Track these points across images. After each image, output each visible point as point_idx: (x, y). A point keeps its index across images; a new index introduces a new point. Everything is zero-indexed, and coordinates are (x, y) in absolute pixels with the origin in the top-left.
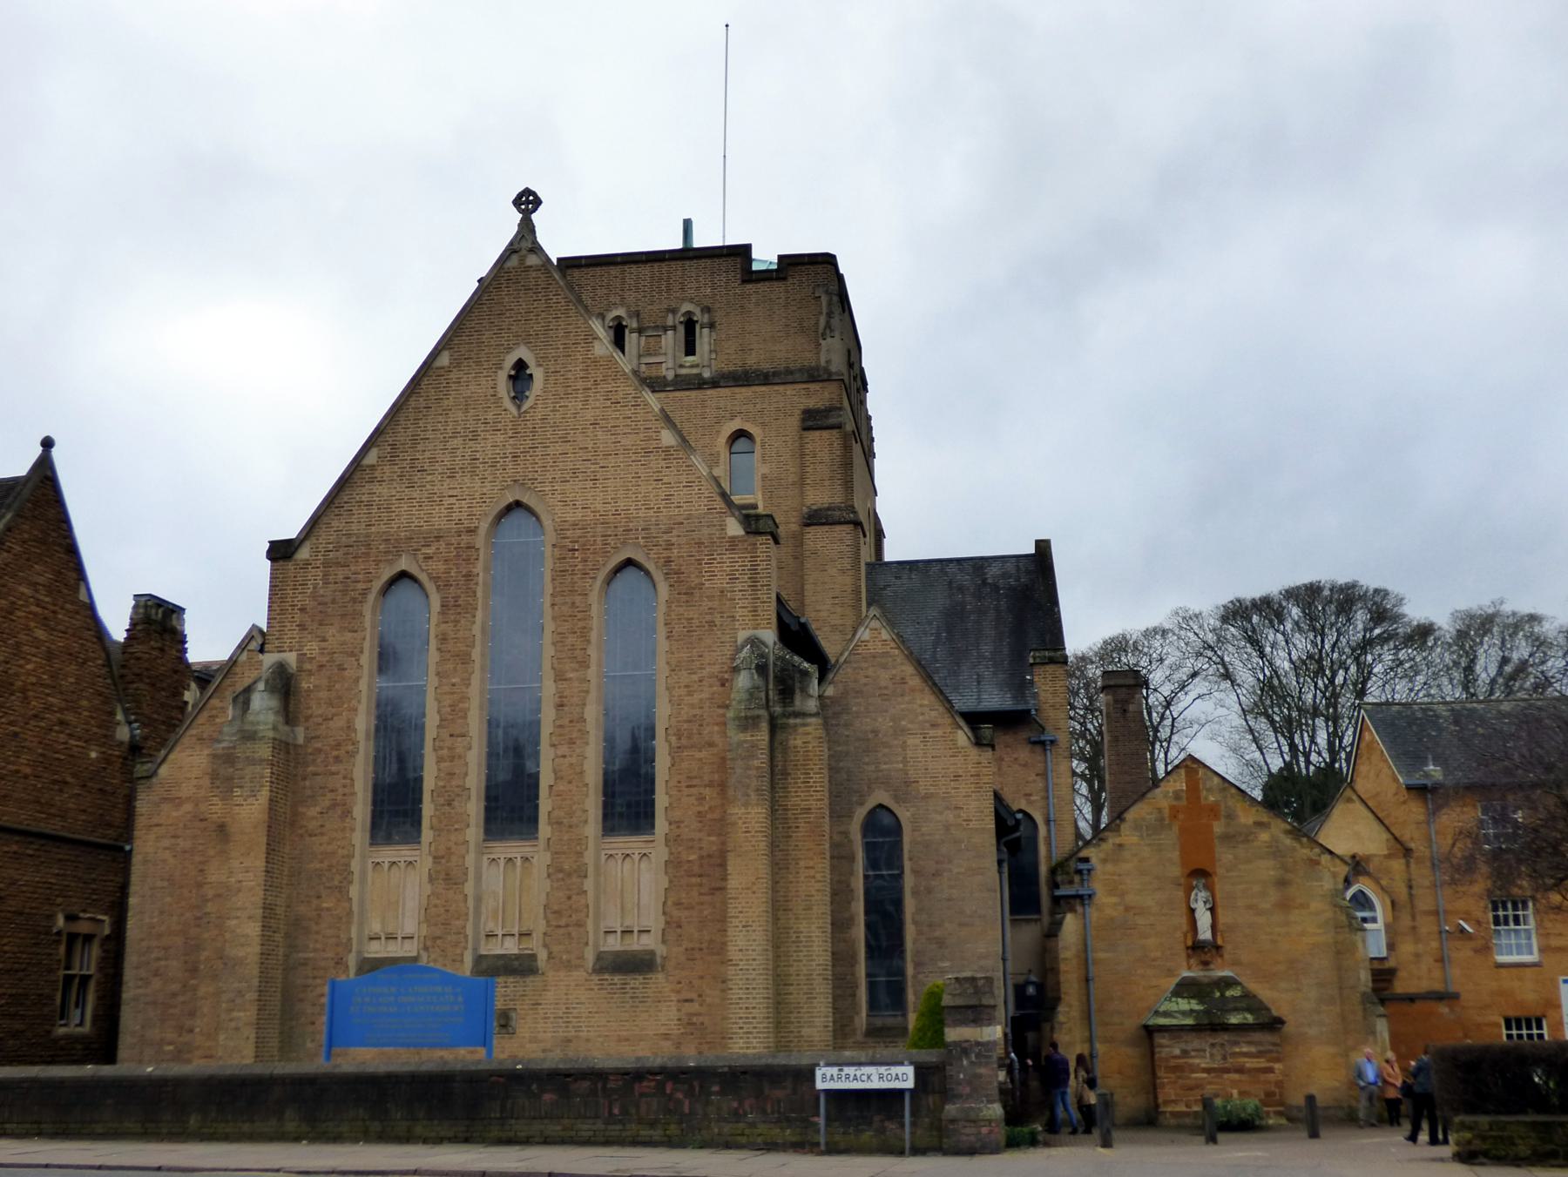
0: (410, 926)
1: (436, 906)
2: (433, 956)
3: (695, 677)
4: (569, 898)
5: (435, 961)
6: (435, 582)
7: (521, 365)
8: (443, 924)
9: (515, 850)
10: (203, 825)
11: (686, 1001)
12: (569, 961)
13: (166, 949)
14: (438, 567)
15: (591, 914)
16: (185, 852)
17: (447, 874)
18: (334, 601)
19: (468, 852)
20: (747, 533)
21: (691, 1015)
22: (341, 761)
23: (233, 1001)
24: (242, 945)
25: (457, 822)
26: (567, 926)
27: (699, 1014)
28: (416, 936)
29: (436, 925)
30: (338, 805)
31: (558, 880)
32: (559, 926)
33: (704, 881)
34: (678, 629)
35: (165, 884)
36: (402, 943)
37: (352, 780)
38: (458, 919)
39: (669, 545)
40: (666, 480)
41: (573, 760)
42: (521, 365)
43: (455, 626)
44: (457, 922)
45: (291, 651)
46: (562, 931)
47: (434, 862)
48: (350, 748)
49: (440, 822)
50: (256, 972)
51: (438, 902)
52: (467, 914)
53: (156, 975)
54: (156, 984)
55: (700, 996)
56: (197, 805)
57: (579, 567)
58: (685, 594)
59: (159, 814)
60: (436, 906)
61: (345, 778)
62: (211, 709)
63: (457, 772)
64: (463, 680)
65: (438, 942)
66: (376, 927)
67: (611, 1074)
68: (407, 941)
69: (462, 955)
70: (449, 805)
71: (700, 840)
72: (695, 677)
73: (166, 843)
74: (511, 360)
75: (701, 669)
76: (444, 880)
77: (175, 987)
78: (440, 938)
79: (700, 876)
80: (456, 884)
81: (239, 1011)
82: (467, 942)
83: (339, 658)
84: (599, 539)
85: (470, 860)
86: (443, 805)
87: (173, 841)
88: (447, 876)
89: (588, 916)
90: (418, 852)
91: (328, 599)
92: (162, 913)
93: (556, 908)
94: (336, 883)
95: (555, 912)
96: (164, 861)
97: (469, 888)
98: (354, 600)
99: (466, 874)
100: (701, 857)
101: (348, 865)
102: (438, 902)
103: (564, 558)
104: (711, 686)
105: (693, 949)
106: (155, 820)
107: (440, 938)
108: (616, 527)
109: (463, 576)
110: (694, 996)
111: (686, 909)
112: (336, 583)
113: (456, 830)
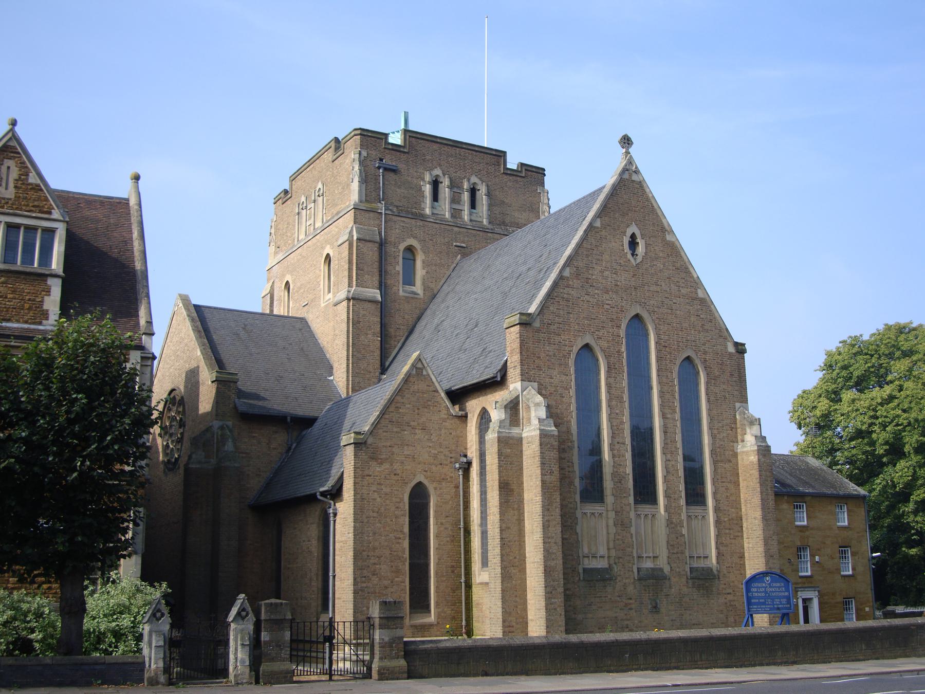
0: (603, 551)
1: (618, 540)
2: (619, 569)
4: (677, 538)
5: (620, 570)
7: (633, 236)
8: (622, 550)
9: (647, 510)
10: (396, 478)
11: (728, 594)
12: (679, 572)
15: (687, 547)
17: (622, 522)
19: (631, 510)
20: (737, 352)
21: (730, 601)
22: (566, 452)
23: (551, 593)
24: (553, 559)
25: (624, 493)
26: (677, 553)
27: (734, 601)
28: (606, 556)
34: (712, 398)
35: (375, 515)
38: (629, 547)
39: (705, 353)
41: (673, 463)
42: (633, 236)
43: (615, 380)
44: (629, 549)
45: (535, 382)
46: (675, 556)
48: (570, 444)
50: (561, 576)
51: (619, 537)
54: (375, 580)
55: (734, 591)
56: (392, 465)
57: (668, 356)
59: (369, 469)
61: (568, 462)
62: (396, 403)
64: (621, 412)
65: (621, 559)
68: (648, 559)
69: (632, 567)
70: (620, 482)
71: (728, 510)
73: (374, 488)
74: (629, 233)
76: (621, 525)
77: (386, 583)
78: (621, 558)
79: (730, 529)
81: (555, 598)
82: (634, 560)
83: (560, 390)
84: (676, 343)
85: (632, 515)
87: (379, 486)
88: (622, 524)
89: (685, 548)
90: (603, 508)
91: (550, 354)
92: (374, 534)
94: (569, 524)
95: (671, 546)
96: (374, 499)
97: (633, 530)
99: (631, 522)
100: (729, 520)
101: (575, 513)
102: (619, 537)
104: (727, 430)
105: (729, 567)
106: (366, 472)
107: (621, 558)
110: (731, 591)
112: (554, 344)
113: (625, 497)
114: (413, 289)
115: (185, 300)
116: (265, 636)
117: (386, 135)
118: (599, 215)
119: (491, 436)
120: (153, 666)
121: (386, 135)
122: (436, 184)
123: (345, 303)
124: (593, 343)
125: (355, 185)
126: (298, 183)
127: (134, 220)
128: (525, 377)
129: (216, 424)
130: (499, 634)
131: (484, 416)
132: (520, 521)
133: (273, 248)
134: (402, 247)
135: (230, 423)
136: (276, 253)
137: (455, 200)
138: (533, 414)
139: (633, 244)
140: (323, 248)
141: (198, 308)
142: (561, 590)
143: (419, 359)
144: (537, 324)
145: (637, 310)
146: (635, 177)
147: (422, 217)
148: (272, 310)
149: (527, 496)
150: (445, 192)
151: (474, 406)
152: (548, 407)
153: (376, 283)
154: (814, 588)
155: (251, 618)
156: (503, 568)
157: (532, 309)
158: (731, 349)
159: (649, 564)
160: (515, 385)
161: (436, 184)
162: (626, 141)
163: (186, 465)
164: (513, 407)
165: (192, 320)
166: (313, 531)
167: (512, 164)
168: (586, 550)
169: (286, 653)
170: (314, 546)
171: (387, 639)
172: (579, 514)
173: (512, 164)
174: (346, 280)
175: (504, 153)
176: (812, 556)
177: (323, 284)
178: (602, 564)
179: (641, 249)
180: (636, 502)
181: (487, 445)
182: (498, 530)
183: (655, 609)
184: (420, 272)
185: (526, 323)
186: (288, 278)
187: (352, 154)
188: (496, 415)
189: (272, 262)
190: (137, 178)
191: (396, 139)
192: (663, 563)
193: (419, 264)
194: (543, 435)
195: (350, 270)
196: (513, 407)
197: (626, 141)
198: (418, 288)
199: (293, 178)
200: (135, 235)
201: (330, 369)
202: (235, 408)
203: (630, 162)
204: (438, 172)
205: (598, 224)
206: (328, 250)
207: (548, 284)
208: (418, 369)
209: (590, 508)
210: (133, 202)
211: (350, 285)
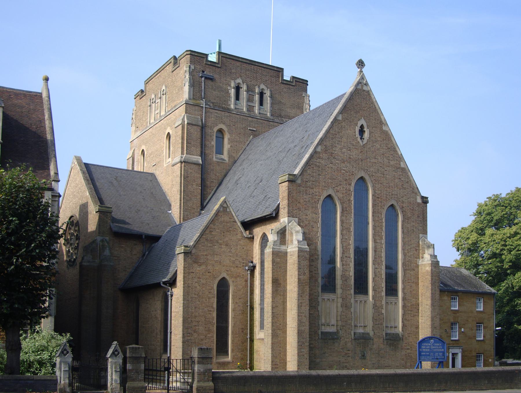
0: (333, 321)
1: (343, 315)
2: (343, 332)
3: (409, 247)
4: (379, 315)
5: (343, 334)
6: (340, 201)
7: (362, 127)
8: (345, 321)
9: (361, 298)
10: (209, 274)
11: (408, 349)
12: (379, 336)
13: (198, 322)
14: (341, 195)
15: (385, 321)
16: (203, 284)
17: (346, 305)
18: (309, 201)
19: (352, 298)
20: (423, 202)
21: (409, 353)
22: (314, 261)
23: (301, 346)
24: (303, 326)
25: (348, 287)
26: (379, 324)
27: (411, 353)
28: (336, 325)
29: (343, 322)
30: (313, 277)
31: (376, 309)
32: (376, 324)
33: (412, 313)
34: (405, 231)
35: (196, 296)
36: (359, 328)
37: (317, 268)
38: (350, 320)
39: (403, 202)
40: (402, 179)
41: (379, 270)
42: (362, 127)
43: (346, 218)
44: (349, 321)
45: (296, 218)
46: (377, 326)
47: (342, 300)
48: (316, 257)
49: (344, 287)
50: (308, 336)
51: (344, 314)
52: (352, 319)
53: (195, 332)
54: (195, 335)
55: (411, 348)
56: (207, 266)
57: (380, 204)
58: (407, 219)
59: (192, 268)
60: (343, 315)
61: (315, 267)
62: (210, 228)
63: (348, 270)
64: (348, 238)
65: (344, 327)
66: (323, 321)
67: (105, 379)
68: (360, 327)
69: (351, 332)
70: (346, 281)
71: (411, 300)
72: (409, 247)
73: (196, 280)
74: (359, 125)
75: (411, 245)
76: (345, 306)
77: (202, 337)
78: (345, 326)
79: (411, 311)
80: (349, 308)
81: (303, 349)
82: (352, 328)
83: (312, 223)
84: (385, 195)
85: (352, 301)
86: (344, 281)
87: (199, 279)
88: (346, 306)
89: (384, 321)
90: (335, 296)
91: (307, 200)
92: (196, 308)
93: (375, 318)
94: (314, 305)
95: (375, 320)
96: (196, 287)
97: (352, 310)
98: (315, 202)
99: (351, 305)
100: (411, 305)
101: (318, 299)
102: (344, 314)
103: (376, 200)
104: (413, 251)
105: (409, 333)
106: (191, 271)
107: (345, 326)
108: (389, 192)
109: (348, 200)
110: (410, 348)
111: (408, 321)
112: (309, 194)
113: (348, 290)
114: (222, 157)
115: (79, 160)
116: (129, 366)
117: (207, 55)
118: (341, 112)
119: (268, 250)
120: (62, 382)
121: (207, 55)
122: (238, 89)
123: (179, 165)
124: (333, 195)
125: (186, 88)
126: (150, 85)
127: (46, 107)
128: (291, 215)
129: (99, 238)
130: (269, 369)
131: (264, 238)
132: (284, 302)
133: (134, 128)
134: (216, 129)
135: (107, 238)
136: (136, 131)
137: (250, 99)
138: (294, 237)
139: (362, 131)
140: (166, 129)
141: (86, 165)
142: (307, 344)
143: (225, 202)
144: (299, 181)
145: (362, 174)
146: (365, 88)
147: (228, 110)
148: (133, 168)
149: (289, 288)
150: (244, 94)
151: (258, 231)
152: (304, 234)
153: (199, 152)
154: (459, 347)
155: (121, 355)
156: (273, 330)
157: (296, 172)
158: (419, 200)
159: (361, 330)
160: (284, 219)
161: (238, 89)
162: (361, 64)
163: (81, 263)
164: (282, 233)
165: (83, 173)
166: (158, 305)
167: (287, 77)
168: (323, 321)
169: (141, 376)
170: (159, 314)
171: (202, 370)
172: (320, 299)
173: (287, 77)
174: (180, 150)
175: (282, 69)
176: (460, 328)
177: (165, 152)
178: (333, 329)
179: (366, 135)
180: (355, 293)
181: (266, 256)
182: (270, 308)
183: (363, 357)
184: (227, 146)
185: (292, 180)
186: (143, 147)
187: (184, 67)
188: (272, 238)
189: (133, 137)
190: (47, 79)
191: (213, 58)
192: (369, 330)
193: (226, 140)
194: (300, 251)
195: (183, 143)
196: (282, 233)
197: (361, 64)
198: (225, 156)
199: (147, 82)
200: (47, 117)
201: (169, 206)
202: (111, 228)
203: (363, 78)
204: (239, 81)
205: (340, 118)
206: (169, 130)
207: (307, 156)
208: (224, 208)
209: (327, 296)
210: (44, 95)
211: (182, 153)
